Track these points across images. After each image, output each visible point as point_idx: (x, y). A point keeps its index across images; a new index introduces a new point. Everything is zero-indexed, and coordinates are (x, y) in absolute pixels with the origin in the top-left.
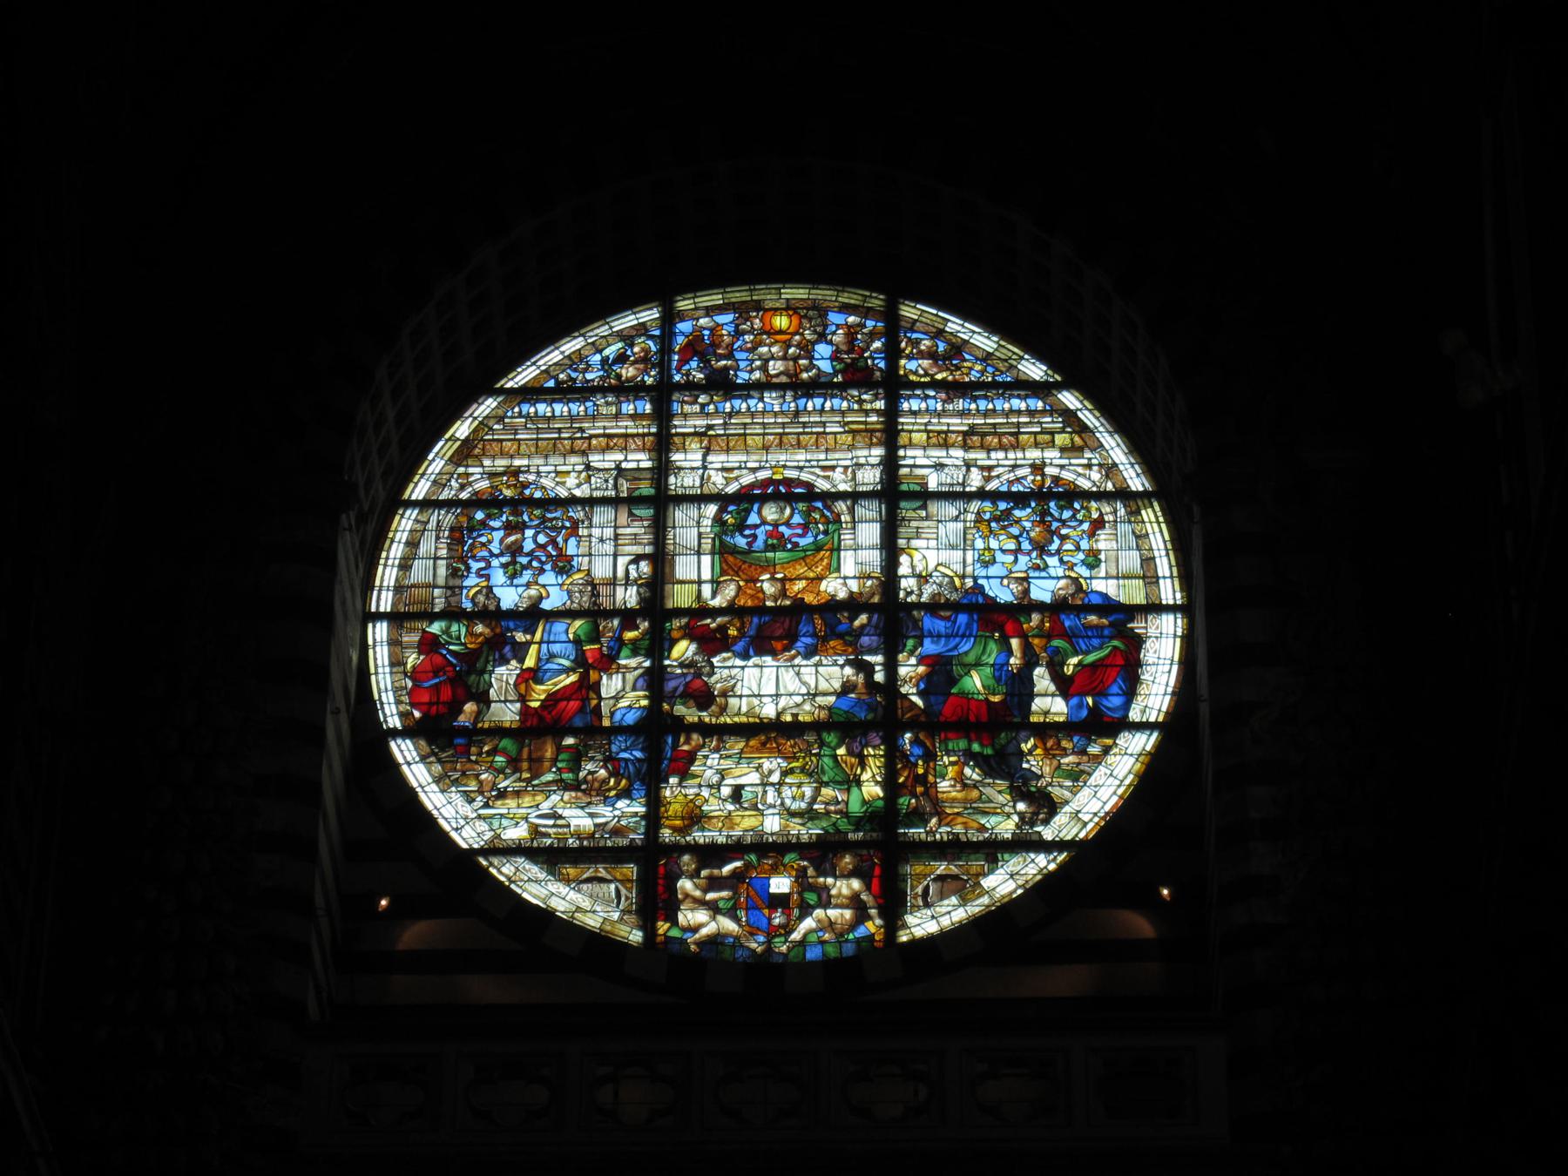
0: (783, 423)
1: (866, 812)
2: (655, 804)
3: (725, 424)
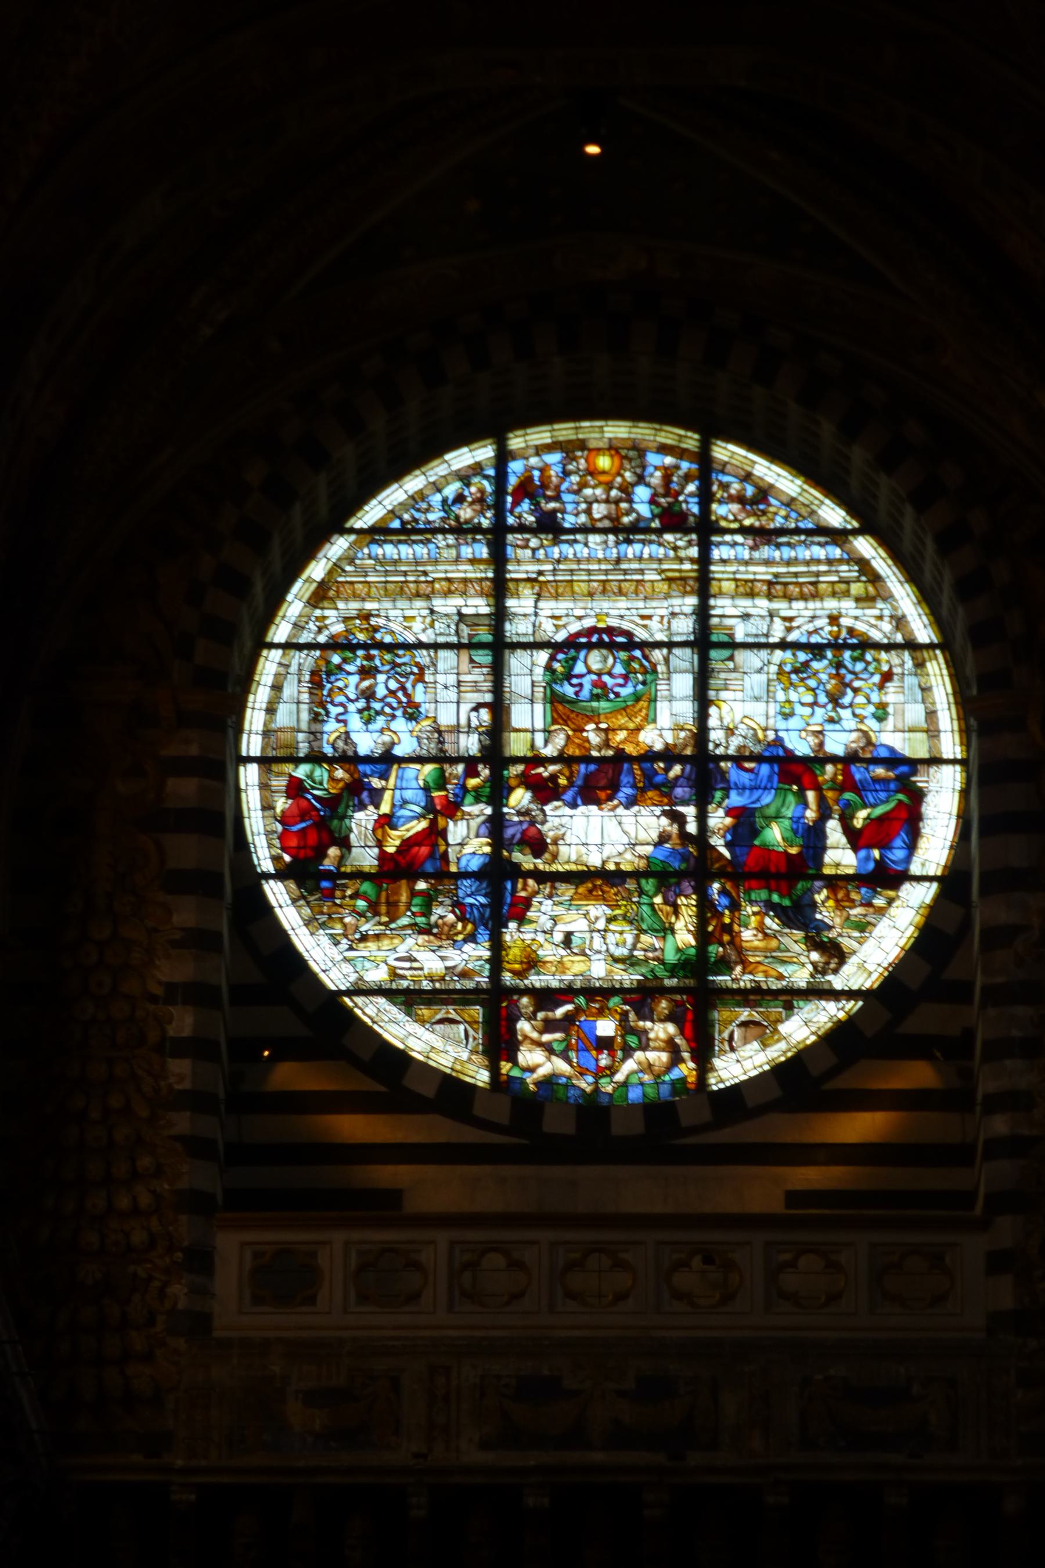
0: (606, 570)
1: (679, 960)
2: (497, 946)
3: (555, 570)
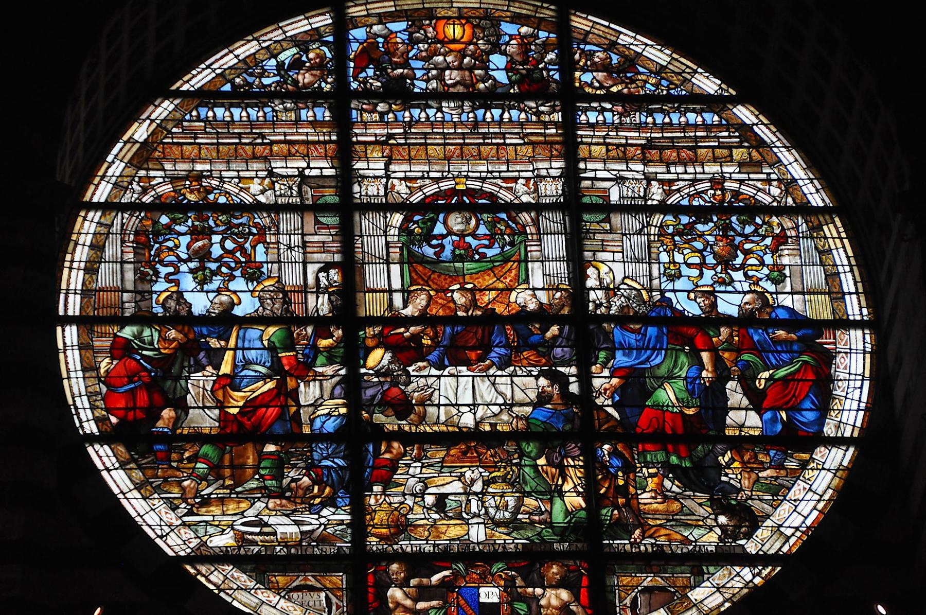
1: (569, 522)
